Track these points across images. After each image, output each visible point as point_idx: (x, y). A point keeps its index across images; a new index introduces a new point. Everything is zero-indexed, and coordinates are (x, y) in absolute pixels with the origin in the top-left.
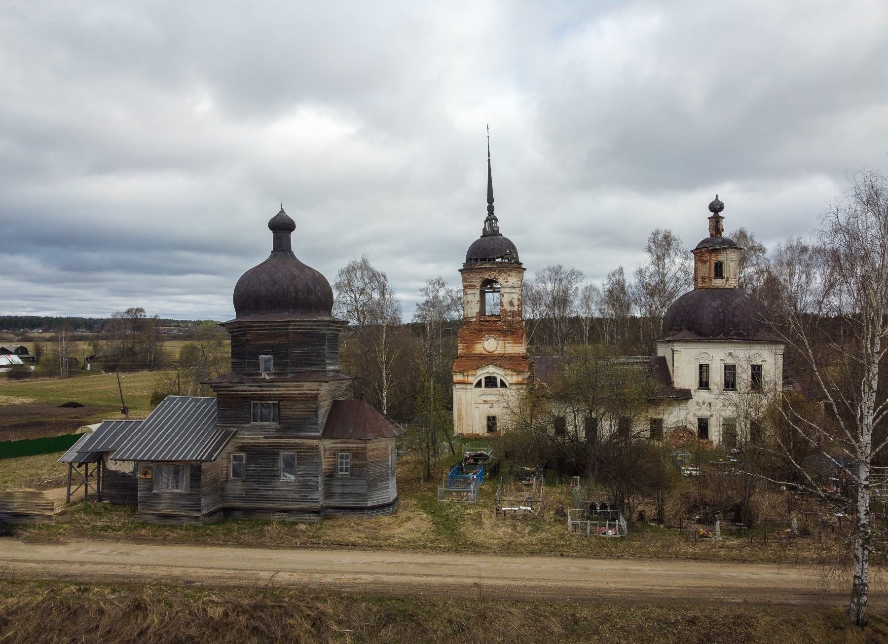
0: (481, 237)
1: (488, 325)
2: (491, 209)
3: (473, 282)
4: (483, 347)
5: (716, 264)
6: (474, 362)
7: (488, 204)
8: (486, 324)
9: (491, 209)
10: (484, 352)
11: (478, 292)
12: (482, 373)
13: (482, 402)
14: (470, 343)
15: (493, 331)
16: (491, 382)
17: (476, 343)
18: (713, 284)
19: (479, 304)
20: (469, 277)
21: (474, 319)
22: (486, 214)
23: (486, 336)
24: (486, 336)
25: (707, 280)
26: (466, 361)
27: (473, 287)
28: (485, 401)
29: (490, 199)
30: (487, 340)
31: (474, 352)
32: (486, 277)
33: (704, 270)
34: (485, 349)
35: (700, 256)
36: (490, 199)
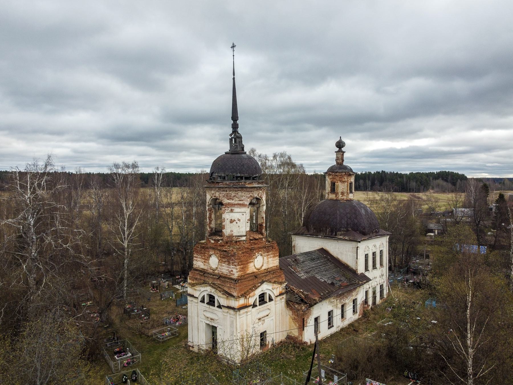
0: (226, 153)
1: (257, 243)
2: (235, 127)
3: (242, 200)
4: (254, 266)
5: (350, 183)
6: (251, 283)
7: (232, 122)
8: (256, 242)
9: (235, 127)
10: (255, 270)
11: (247, 210)
12: (258, 292)
13: (257, 321)
14: (244, 263)
15: (261, 248)
16: (262, 299)
17: (250, 262)
18: (349, 197)
19: (249, 223)
20: (237, 195)
21: (244, 238)
22: (230, 130)
23: (256, 253)
24: (256, 253)
25: (345, 194)
26: (245, 283)
27: (243, 205)
28: (259, 319)
29: (235, 117)
30: (256, 258)
31: (248, 272)
32: (255, 196)
33: (343, 187)
34: (255, 268)
35: (340, 178)
36: (235, 117)
